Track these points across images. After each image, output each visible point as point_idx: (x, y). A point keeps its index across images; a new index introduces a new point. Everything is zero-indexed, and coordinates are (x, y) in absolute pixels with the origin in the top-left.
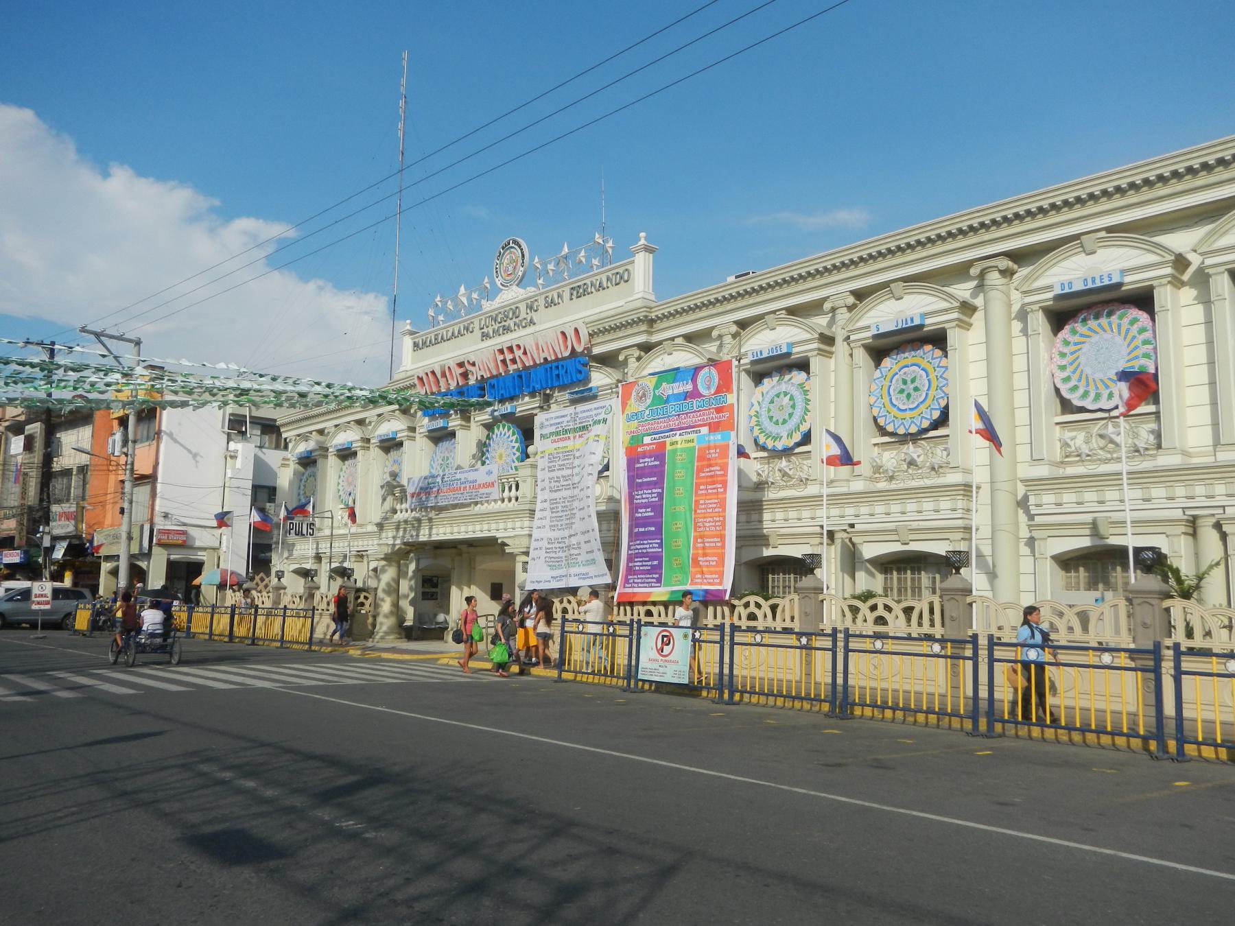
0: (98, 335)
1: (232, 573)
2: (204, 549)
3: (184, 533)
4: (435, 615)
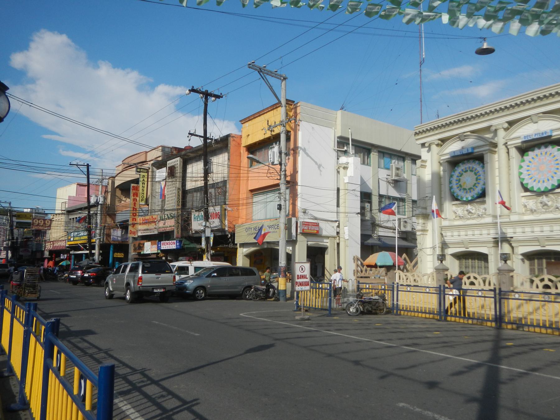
0: (260, 70)
2: (328, 237)
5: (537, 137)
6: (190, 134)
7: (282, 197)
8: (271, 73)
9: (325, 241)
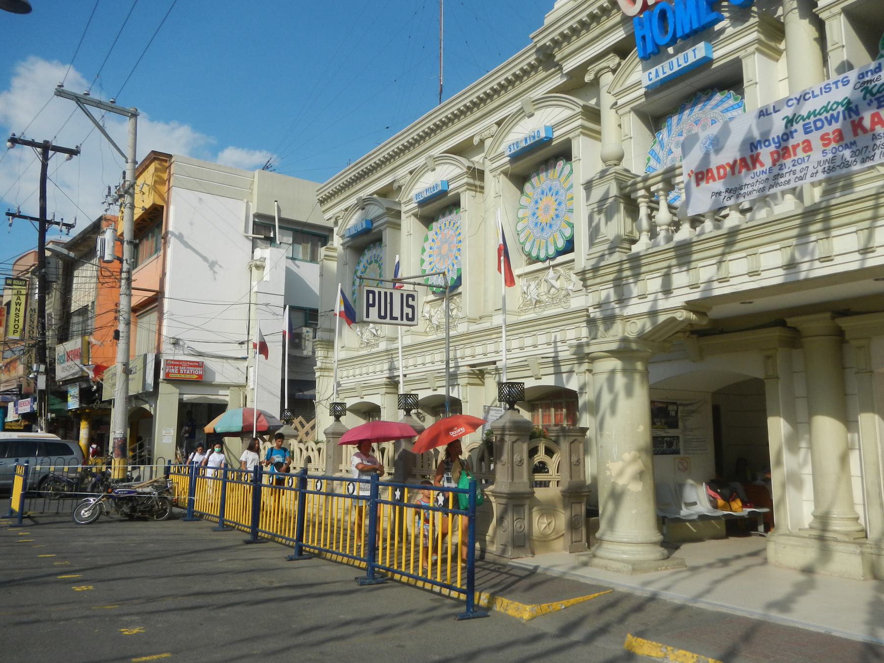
1: (260, 414)
3: (200, 365)
4: (681, 487)
5: (429, 194)
6: (8, 214)
7: (121, 318)
8: (98, 104)
9: (221, 392)
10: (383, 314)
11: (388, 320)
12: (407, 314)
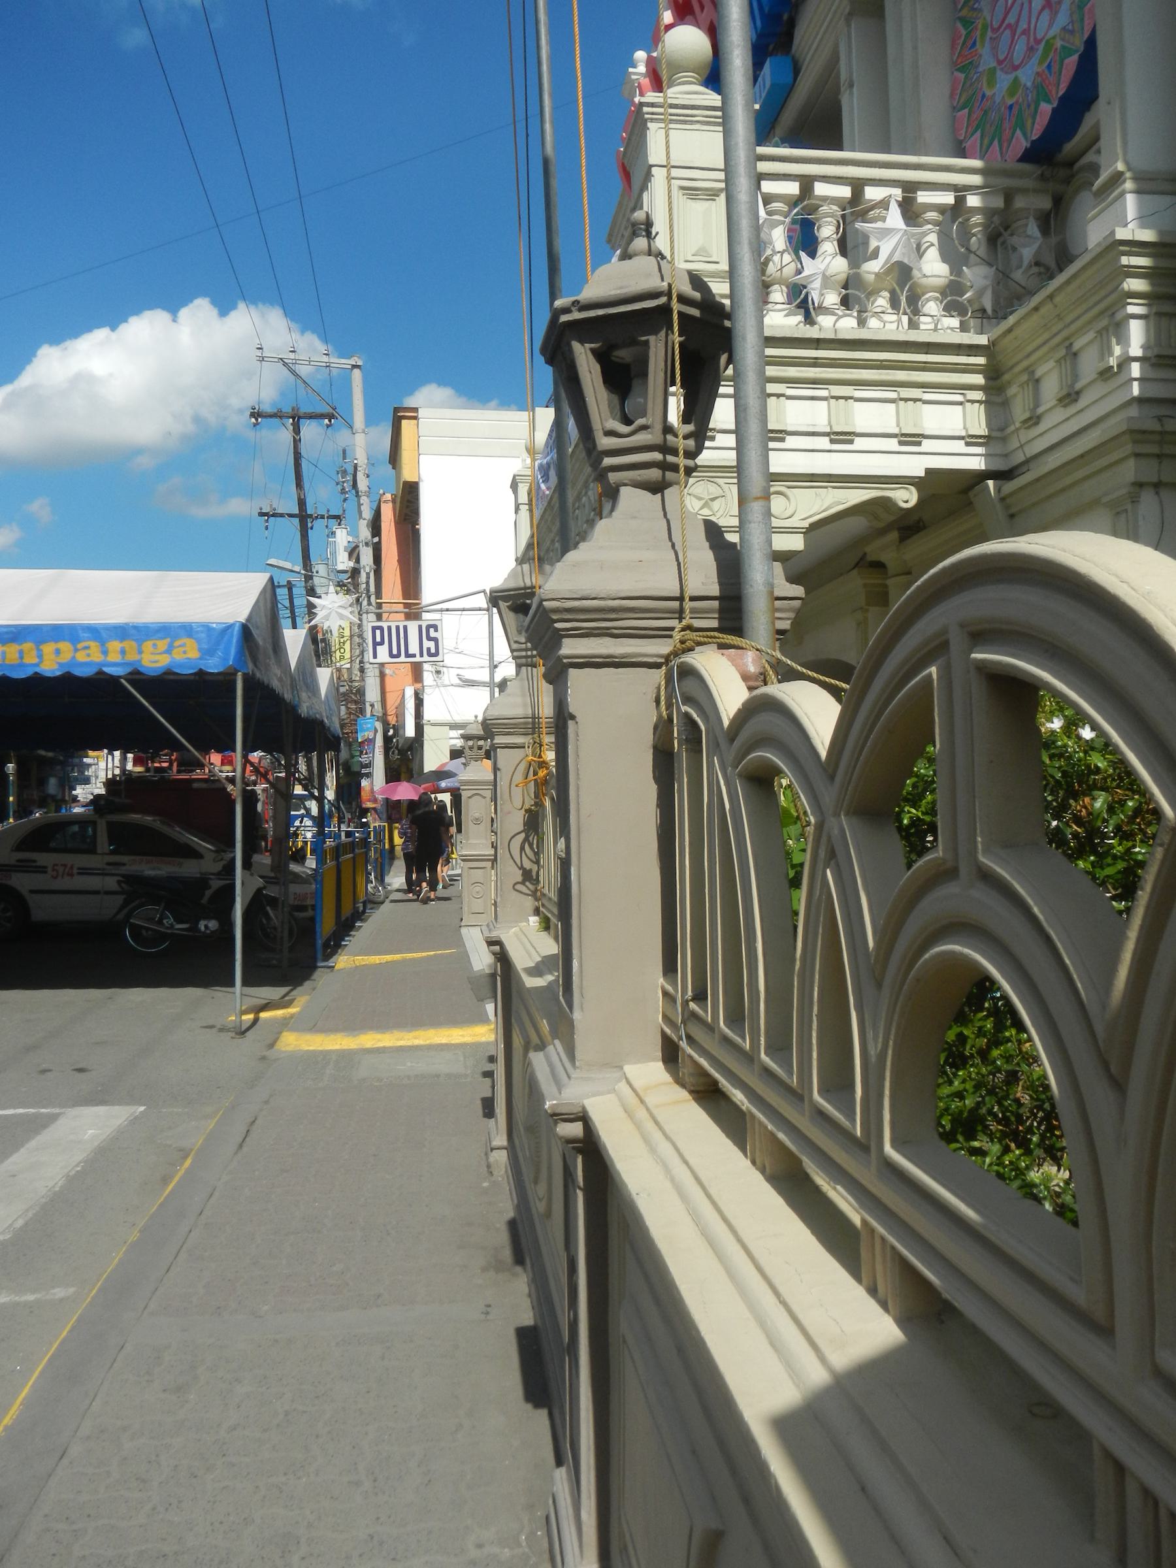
6: (262, 514)
10: (395, 652)
11: (403, 658)
12: (428, 649)
